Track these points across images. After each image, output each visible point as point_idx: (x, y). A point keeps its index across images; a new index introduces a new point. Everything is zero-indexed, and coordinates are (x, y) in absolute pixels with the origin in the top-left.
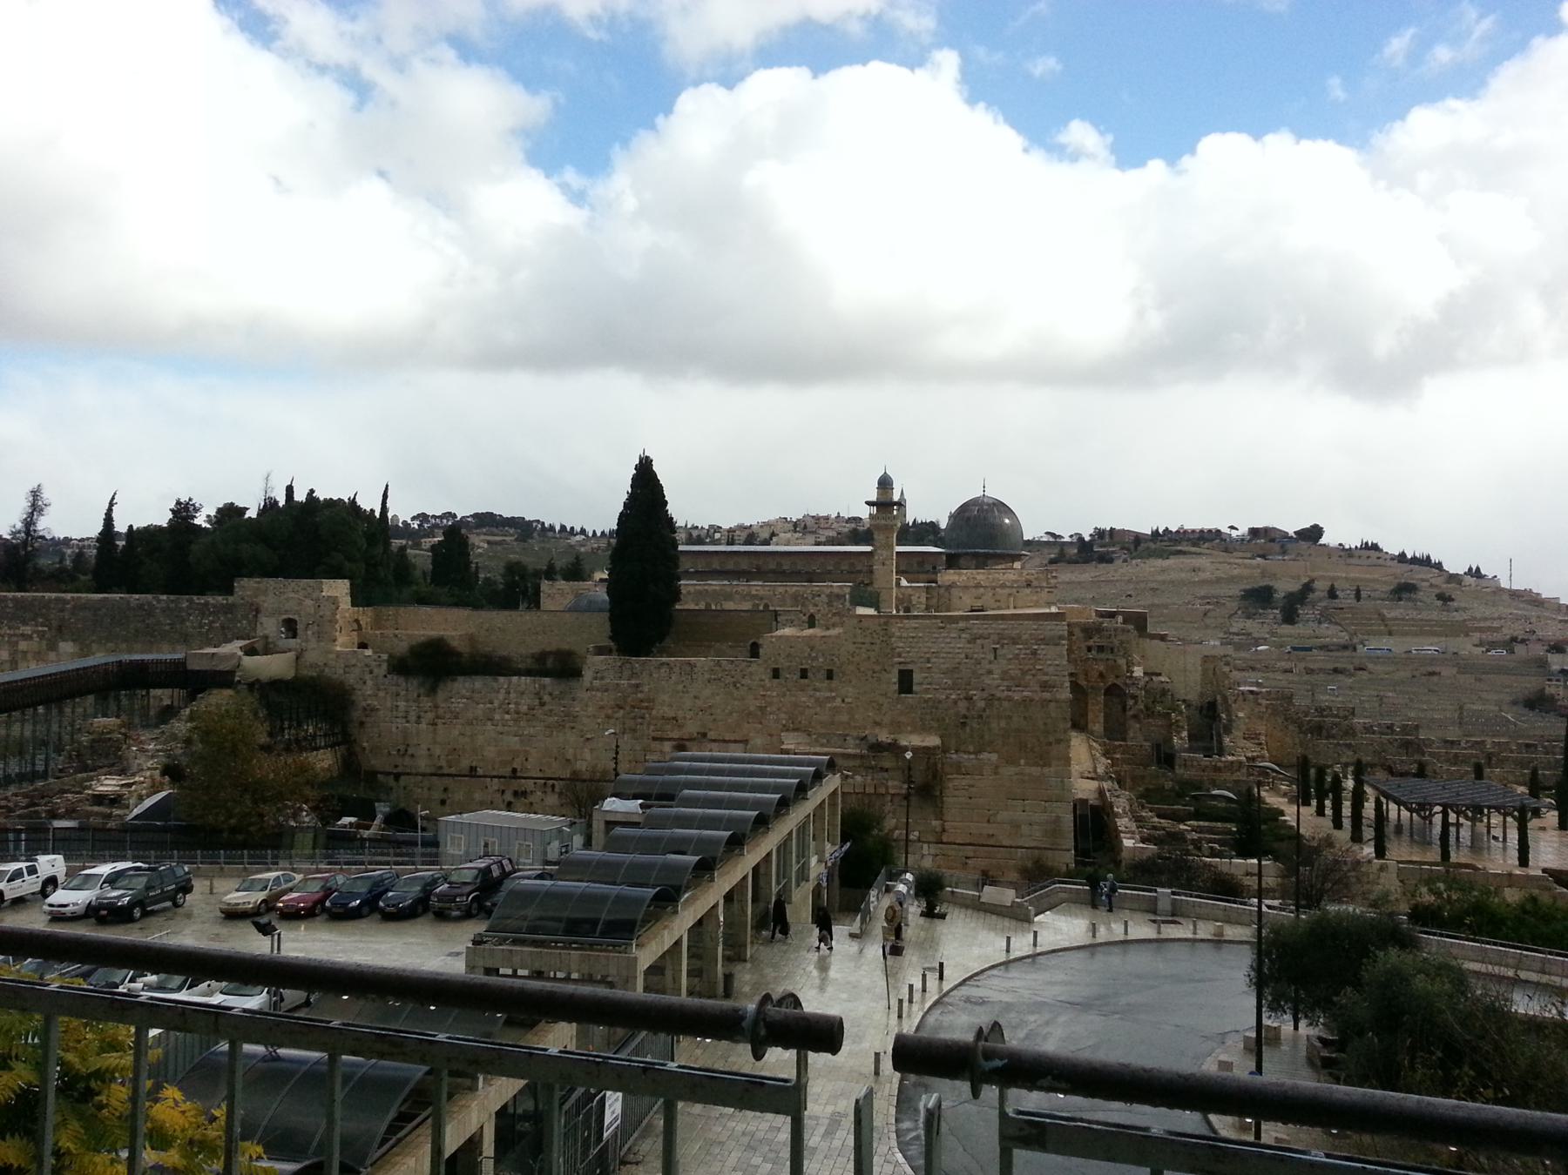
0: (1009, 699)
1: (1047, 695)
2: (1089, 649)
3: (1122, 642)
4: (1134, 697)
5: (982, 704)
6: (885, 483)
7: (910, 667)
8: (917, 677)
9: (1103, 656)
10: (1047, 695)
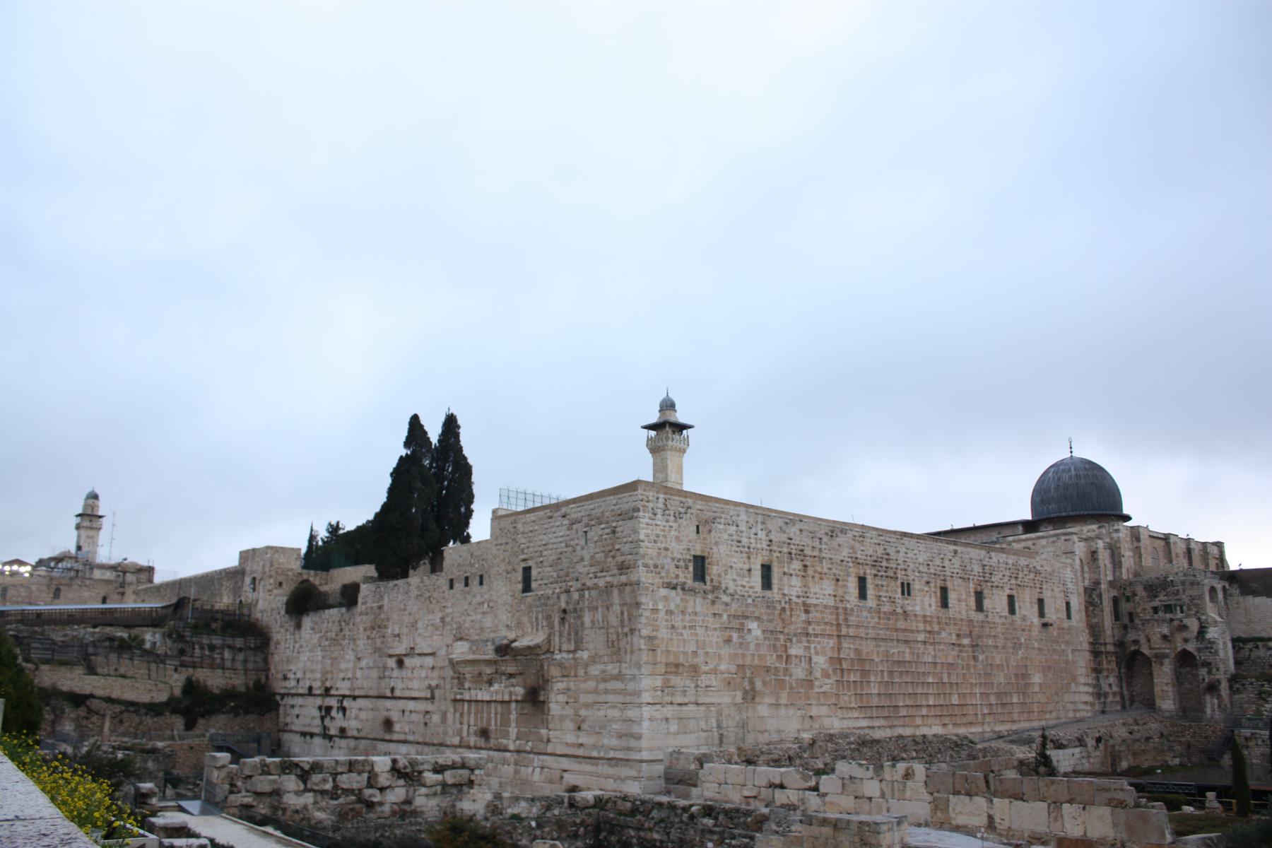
0: (596, 587)
1: (623, 579)
2: (1155, 610)
3: (1192, 598)
4: (1207, 664)
5: (576, 596)
7: (530, 563)
8: (534, 573)
9: (1169, 616)
10: (623, 579)
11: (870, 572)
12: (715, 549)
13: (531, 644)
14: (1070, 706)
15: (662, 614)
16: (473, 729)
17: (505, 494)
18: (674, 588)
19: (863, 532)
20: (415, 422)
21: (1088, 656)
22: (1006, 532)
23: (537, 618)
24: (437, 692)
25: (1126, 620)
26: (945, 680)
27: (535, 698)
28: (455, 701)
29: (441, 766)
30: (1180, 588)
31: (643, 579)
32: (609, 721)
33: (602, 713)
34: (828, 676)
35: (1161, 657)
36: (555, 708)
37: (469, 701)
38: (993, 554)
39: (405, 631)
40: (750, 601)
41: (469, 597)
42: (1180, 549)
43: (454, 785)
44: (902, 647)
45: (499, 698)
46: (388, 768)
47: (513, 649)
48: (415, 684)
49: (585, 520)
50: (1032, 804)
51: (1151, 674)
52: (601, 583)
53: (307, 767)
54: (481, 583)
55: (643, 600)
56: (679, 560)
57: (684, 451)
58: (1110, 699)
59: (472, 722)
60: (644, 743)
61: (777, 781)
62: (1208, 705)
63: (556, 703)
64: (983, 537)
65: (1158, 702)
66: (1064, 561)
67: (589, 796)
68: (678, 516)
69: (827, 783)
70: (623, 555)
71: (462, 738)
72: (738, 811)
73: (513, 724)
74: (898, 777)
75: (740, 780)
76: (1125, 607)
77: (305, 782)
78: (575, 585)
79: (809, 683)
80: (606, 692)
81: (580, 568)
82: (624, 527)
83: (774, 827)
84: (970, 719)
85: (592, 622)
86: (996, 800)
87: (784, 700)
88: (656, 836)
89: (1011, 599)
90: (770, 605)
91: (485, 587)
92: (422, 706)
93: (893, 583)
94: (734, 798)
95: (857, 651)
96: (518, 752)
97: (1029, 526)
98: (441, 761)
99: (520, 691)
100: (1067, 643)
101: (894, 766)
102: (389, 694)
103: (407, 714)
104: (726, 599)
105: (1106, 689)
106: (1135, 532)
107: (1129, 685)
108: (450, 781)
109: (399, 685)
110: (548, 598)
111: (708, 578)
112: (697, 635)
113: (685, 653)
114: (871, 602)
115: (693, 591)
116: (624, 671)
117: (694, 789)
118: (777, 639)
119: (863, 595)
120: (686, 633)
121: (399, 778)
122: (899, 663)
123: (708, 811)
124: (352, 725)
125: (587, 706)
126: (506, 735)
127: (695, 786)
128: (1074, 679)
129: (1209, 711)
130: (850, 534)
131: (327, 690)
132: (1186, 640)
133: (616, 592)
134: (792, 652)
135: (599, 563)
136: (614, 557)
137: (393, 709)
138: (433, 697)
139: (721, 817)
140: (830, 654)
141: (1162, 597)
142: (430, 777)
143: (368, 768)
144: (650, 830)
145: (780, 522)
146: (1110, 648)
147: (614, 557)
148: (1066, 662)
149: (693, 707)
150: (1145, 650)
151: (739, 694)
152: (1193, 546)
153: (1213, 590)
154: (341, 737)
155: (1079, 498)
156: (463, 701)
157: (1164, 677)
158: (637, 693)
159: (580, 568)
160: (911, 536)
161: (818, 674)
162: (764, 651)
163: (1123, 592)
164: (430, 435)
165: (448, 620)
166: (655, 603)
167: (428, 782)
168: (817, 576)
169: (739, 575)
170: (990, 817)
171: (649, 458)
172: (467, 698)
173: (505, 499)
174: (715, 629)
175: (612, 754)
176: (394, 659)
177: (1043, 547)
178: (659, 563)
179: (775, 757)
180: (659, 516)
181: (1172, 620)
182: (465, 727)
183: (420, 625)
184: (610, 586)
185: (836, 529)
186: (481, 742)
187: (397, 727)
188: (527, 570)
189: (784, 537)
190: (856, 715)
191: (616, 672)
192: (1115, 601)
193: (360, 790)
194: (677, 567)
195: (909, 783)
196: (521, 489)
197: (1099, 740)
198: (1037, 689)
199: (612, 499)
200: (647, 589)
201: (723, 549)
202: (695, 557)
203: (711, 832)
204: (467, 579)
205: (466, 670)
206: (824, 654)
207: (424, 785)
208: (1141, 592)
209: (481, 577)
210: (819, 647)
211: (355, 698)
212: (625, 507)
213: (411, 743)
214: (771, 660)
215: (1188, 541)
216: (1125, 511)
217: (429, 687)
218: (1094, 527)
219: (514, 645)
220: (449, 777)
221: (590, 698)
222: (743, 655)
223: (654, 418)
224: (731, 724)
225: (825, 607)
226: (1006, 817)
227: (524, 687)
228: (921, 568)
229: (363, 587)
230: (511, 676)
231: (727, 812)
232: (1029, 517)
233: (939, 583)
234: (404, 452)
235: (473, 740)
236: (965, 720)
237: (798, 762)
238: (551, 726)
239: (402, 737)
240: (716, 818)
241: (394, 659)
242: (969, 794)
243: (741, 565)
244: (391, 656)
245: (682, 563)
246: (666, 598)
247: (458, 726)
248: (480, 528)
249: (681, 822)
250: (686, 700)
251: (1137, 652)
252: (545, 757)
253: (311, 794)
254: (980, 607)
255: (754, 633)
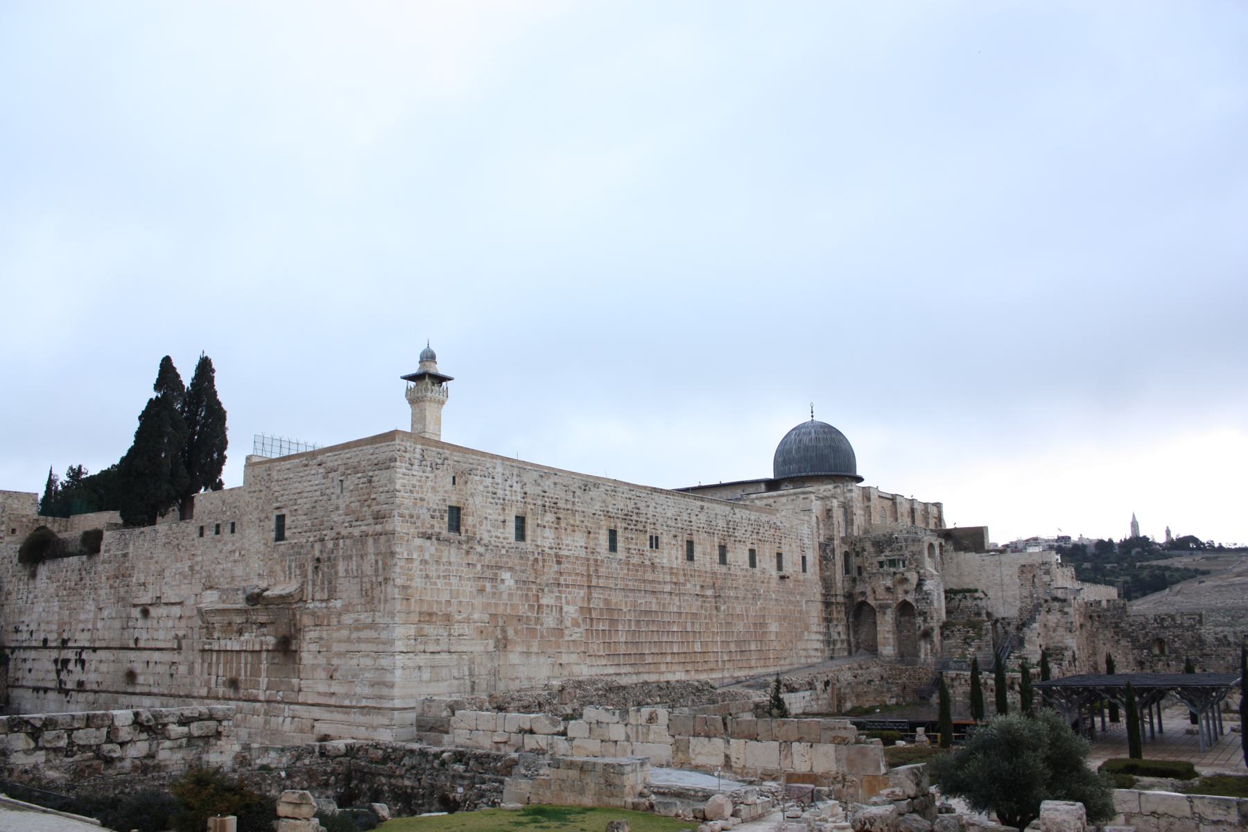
0: (350, 536)
1: (379, 528)
2: (881, 564)
3: (913, 554)
5: (330, 545)
6: (428, 357)
7: (284, 511)
8: (288, 521)
9: (892, 570)
10: (379, 528)
11: (620, 525)
12: (471, 501)
13: (283, 593)
14: (803, 653)
15: (416, 564)
16: (220, 680)
17: (260, 441)
18: (429, 538)
19: (615, 486)
20: (167, 365)
21: (820, 606)
22: (750, 490)
23: (290, 567)
24: (184, 643)
25: (855, 573)
26: (689, 629)
27: (286, 648)
28: (203, 651)
29: (187, 718)
30: (904, 544)
31: (398, 529)
32: (361, 670)
33: (354, 662)
34: (578, 625)
35: (884, 608)
36: (307, 658)
37: (218, 651)
38: (737, 510)
39: (151, 579)
40: (504, 551)
41: (220, 545)
42: (904, 509)
43: (200, 737)
44: (649, 598)
45: (250, 648)
46: (130, 722)
47: (264, 598)
48: (161, 635)
49: (342, 469)
50: (765, 744)
51: (875, 623)
52: (356, 532)
53: (38, 724)
54: (233, 531)
55: (398, 549)
56: (435, 511)
57: (443, 403)
58: (839, 646)
59: (221, 673)
60: (396, 692)
61: (527, 727)
62: (923, 650)
63: (308, 653)
64: (728, 494)
65: (880, 648)
66: (801, 519)
67: (340, 744)
68: (434, 467)
69: (574, 727)
70: (378, 504)
71: (210, 689)
72: (488, 756)
73: (264, 674)
74: (643, 720)
75: (491, 727)
76: (855, 562)
77: (36, 740)
78: (330, 534)
79: (559, 632)
80: (359, 640)
81: (335, 517)
82: (380, 477)
83: (523, 771)
84: (711, 665)
85: (347, 571)
86: (732, 741)
87: (535, 649)
88: (407, 783)
89: (752, 552)
90: (523, 556)
91: (237, 535)
92: (167, 657)
93: (642, 536)
94: (485, 743)
95: (607, 602)
96: (268, 702)
97: (771, 485)
98: (187, 713)
99: (271, 641)
100: (802, 594)
101: (639, 711)
102: (132, 645)
103: (151, 665)
104: (480, 549)
105: (835, 636)
106: (866, 494)
107: (856, 632)
108: (196, 734)
109: (144, 636)
110: (302, 547)
111: (462, 529)
112: (450, 584)
113: (438, 603)
114: (621, 554)
115: (448, 540)
116: (377, 620)
117: (446, 736)
118: (529, 589)
119: (613, 548)
120: (440, 583)
121: (141, 731)
122: (646, 612)
123: (459, 757)
124: (91, 678)
125: (340, 655)
126: (256, 685)
127: (447, 733)
128: (807, 628)
129: (922, 656)
130: (602, 489)
131: (64, 642)
132: (906, 592)
133: (370, 540)
134: (544, 601)
135: (354, 512)
136: (369, 506)
137: (136, 661)
138: (180, 648)
139: (471, 763)
140: (580, 604)
141: (887, 553)
142: (175, 730)
143: (107, 723)
144: (402, 777)
145: (535, 475)
146: (841, 599)
147: (369, 506)
148: (801, 612)
149: (445, 656)
150: (871, 601)
151: (491, 642)
152: (916, 506)
153: (931, 546)
154: (79, 691)
155: (817, 460)
156: (212, 651)
157: (886, 625)
158: (391, 642)
159: (335, 517)
160: (661, 491)
161: (568, 623)
162: (516, 601)
163: (854, 549)
164: (182, 378)
165: (197, 568)
166: (410, 553)
167: (173, 735)
168: (570, 528)
169: (493, 526)
170: (727, 757)
171: (407, 408)
172: (216, 648)
173: (259, 446)
174: (469, 579)
175: (364, 703)
176: (139, 609)
177: (784, 504)
178: (414, 513)
179: (525, 703)
180: (416, 467)
181: (895, 573)
182: (214, 678)
183: (167, 573)
184: (364, 535)
185: (589, 484)
186: (230, 693)
187: (141, 679)
188: (281, 519)
189: (538, 490)
190: (604, 662)
191: (369, 620)
192: (847, 555)
193: (98, 746)
194: (433, 517)
195: (653, 727)
196: (277, 436)
197: (827, 683)
198: (773, 638)
199: (369, 449)
200: (402, 538)
201: (478, 500)
202: (450, 507)
203: (462, 777)
204: (218, 526)
205: (216, 619)
206: (574, 603)
207: (169, 739)
208: (869, 547)
209: (233, 524)
210: (569, 597)
211: (95, 650)
212: (382, 457)
213: (155, 695)
214: (523, 610)
215: (912, 501)
216: (859, 473)
217: (176, 637)
218: (830, 487)
219: (265, 594)
220: (195, 729)
221: (343, 647)
222: (496, 605)
223: (414, 369)
224: (483, 671)
225: (577, 558)
226: (741, 756)
227: (275, 637)
228: (669, 523)
229: (106, 534)
230: (262, 625)
231: (477, 758)
232: (772, 477)
233: (686, 537)
234: (154, 395)
235: (221, 691)
236: (706, 667)
237: (547, 708)
238: (302, 676)
239: (146, 689)
240: (467, 764)
241: (139, 609)
242: (708, 736)
243: (495, 517)
244: (135, 606)
245: (437, 514)
246: (421, 549)
247: (206, 677)
248: (232, 474)
249: (433, 768)
250: (438, 649)
251: (864, 603)
252: (297, 707)
253: (43, 752)
254: (723, 560)
255: (507, 583)
